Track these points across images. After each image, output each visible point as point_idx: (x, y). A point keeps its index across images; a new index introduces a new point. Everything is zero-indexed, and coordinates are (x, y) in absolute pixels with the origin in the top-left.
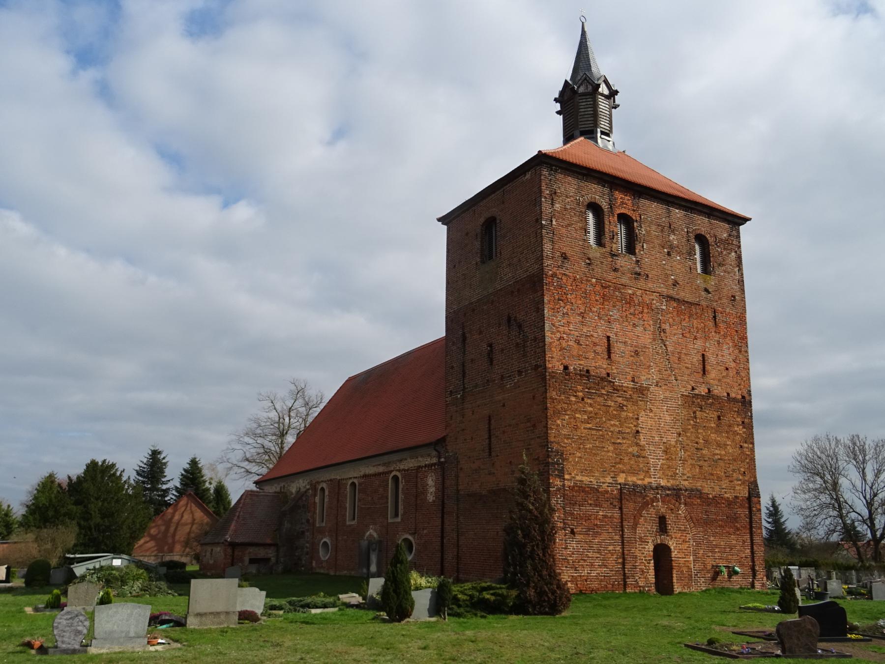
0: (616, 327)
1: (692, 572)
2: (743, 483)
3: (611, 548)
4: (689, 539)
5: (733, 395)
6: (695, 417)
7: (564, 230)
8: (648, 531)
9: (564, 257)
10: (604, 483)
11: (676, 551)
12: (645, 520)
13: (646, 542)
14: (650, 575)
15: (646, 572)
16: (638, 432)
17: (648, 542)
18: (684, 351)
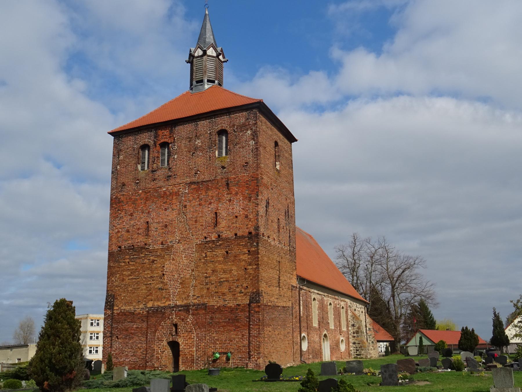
0: (153, 214)
1: (194, 357)
2: (245, 294)
3: (139, 345)
4: (194, 337)
5: (239, 234)
6: (206, 256)
7: (124, 170)
8: (163, 334)
9: (124, 185)
10: (138, 308)
11: (183, 345)
12: (163, 328)
13: (162, 340)
14: (162, 360)
15: (160, 359)
16: (164, 275)
17: (163, 341)
18: (201, 215)
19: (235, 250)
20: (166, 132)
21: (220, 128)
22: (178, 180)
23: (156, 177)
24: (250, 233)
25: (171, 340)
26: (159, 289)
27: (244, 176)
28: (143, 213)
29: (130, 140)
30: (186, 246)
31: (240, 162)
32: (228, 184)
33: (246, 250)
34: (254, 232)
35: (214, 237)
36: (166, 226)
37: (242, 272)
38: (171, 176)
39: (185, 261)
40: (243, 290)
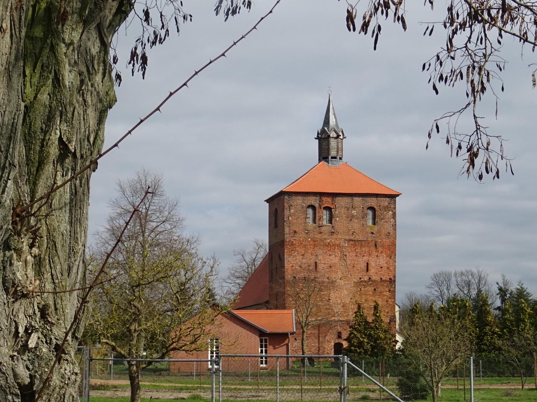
0: (320, 257)
2: (387, 316)
3: (313, 345)
5: (384, 278)
6: (361, 291)
7: (295, 221)
9: (295, 232)
12: (331, 333)
16: (329, 299)
18: (357, 263)
19: (380, 289)
20: (329, 199)
21: (370, 206)
22: (339, 236)
23: (321, 231)
24: (390, 279)
25: (337, 342)
26: (327, 309)
27: (387, 241)
28: (312, 255)
29: (298, 199)
30: (346, 282)
31: (384, 232)
32: (376, 245)
33: (387, 289)
34: (393, 279)
35: (366, 278)
36: (330, 267)
37: (385, 303)
38: (333, 233)
39: (346, 292)
40: (385, 314)
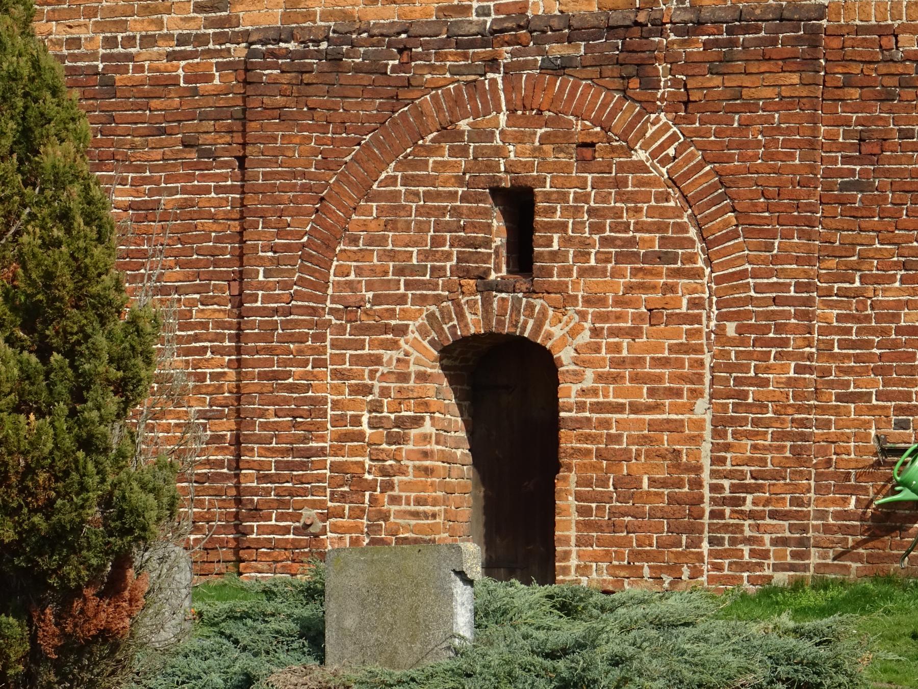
1: (698, 484)
4: (695, 304)
8: (400, 271)
10: (148, 41)
11: (589, 374)
13: (387, 329)
14: (394, 500)
15: (372, 486)
17: (402, 331)
25: (474, 324)
